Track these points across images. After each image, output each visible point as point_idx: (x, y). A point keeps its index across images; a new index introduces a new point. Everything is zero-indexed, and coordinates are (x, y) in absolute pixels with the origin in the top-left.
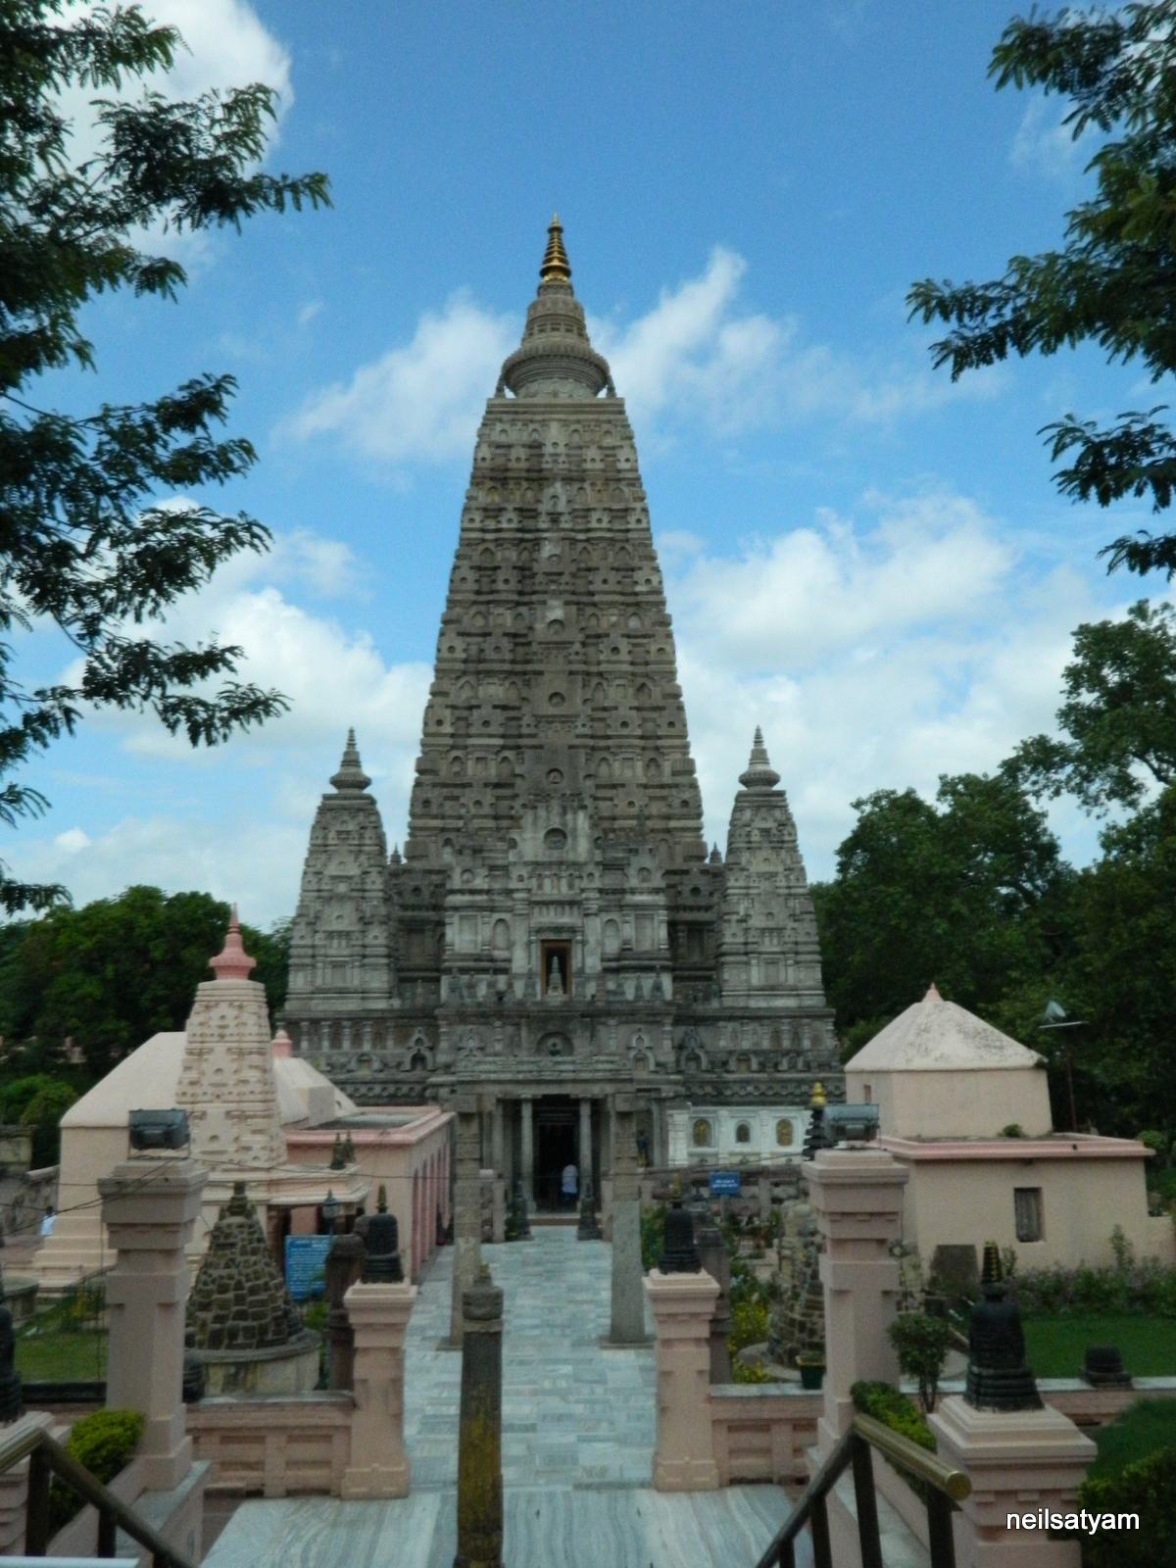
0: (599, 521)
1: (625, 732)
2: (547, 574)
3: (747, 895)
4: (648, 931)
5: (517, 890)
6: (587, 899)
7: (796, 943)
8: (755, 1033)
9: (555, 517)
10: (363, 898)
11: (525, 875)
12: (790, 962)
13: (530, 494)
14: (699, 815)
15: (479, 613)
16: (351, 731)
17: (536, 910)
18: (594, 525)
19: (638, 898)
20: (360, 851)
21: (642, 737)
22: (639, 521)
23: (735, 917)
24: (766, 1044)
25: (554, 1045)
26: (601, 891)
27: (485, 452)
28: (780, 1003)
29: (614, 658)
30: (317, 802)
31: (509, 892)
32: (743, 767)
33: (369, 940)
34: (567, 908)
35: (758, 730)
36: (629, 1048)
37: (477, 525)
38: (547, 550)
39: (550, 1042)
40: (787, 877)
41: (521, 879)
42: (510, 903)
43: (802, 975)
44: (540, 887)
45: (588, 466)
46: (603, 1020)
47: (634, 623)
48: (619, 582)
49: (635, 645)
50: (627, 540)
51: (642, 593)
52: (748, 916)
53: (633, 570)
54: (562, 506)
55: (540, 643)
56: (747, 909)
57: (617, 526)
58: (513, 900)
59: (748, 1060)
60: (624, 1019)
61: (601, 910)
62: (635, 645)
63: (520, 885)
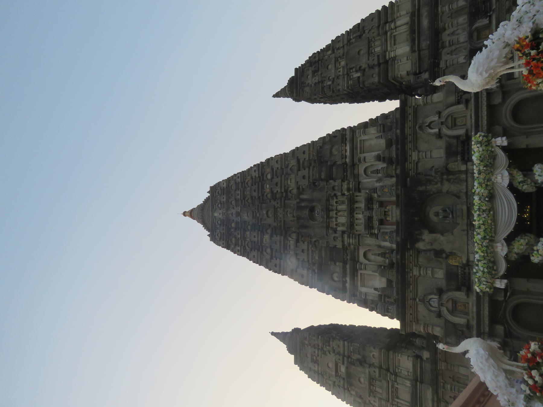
0: (238, 195)
1: (307, 176)
2: (253, 218)
3: (348, 74)
4: (374, 142)
5: (343, 242)
6: (349, 190)
7: (379, 26)
8: (453, 33)
9: (238, 214)
10: (349, 357)
11: (333, 235)
12: (393, 26)
13: (233, 225)
14: (343, 129)
15: (266, 251)
16: (273, 334)
17: (357, 228)
18: (239, 197)
19: (348, 153)
20: (322, 349)
21: (309, 168)
22: (238, 177)
23: (361, 79)
24: (462, 20)
25: (437, 214)
26: (343, 181)
27: (221, 243)
28: (425, 22)
29: (279, 184)
30: (297, 367)
31: (345, 249)
32: (290, 100)
33: (376, 362)
34: (357, 205)
35: (274, 96)
36: (439, 136)
37: (239, 248)
38: (245, 217)
39: (434, 219)
40: (338, 49)
41: (335, 239)
42: (352, 247)
43: (403, 13)
44: (343, 225)
45: (225, 200)
46: (409, 166)
47: (269, 177)
48: (255, 184)
49: (276, 175)
50: (244, 182)
51: (259, 174)
52: (360, 69)
53: (252, 178)
54: (234, 211)
55: (275, 221)
56: (357, 71)
57: (240, 187)
58: (349, 244)
59: (478, 30)
60: (410, 145)
61: (356, 177)
62: (276, 175)
63: (340, 239)
